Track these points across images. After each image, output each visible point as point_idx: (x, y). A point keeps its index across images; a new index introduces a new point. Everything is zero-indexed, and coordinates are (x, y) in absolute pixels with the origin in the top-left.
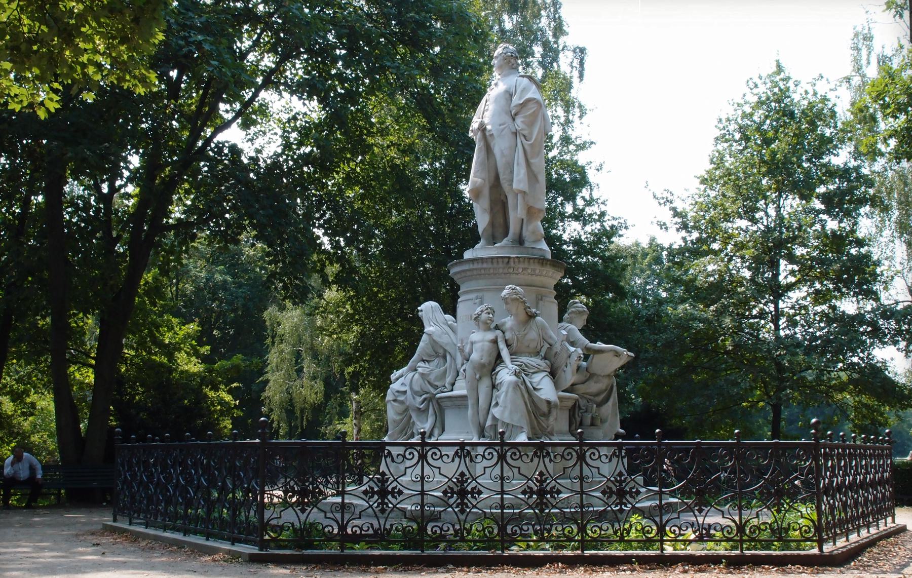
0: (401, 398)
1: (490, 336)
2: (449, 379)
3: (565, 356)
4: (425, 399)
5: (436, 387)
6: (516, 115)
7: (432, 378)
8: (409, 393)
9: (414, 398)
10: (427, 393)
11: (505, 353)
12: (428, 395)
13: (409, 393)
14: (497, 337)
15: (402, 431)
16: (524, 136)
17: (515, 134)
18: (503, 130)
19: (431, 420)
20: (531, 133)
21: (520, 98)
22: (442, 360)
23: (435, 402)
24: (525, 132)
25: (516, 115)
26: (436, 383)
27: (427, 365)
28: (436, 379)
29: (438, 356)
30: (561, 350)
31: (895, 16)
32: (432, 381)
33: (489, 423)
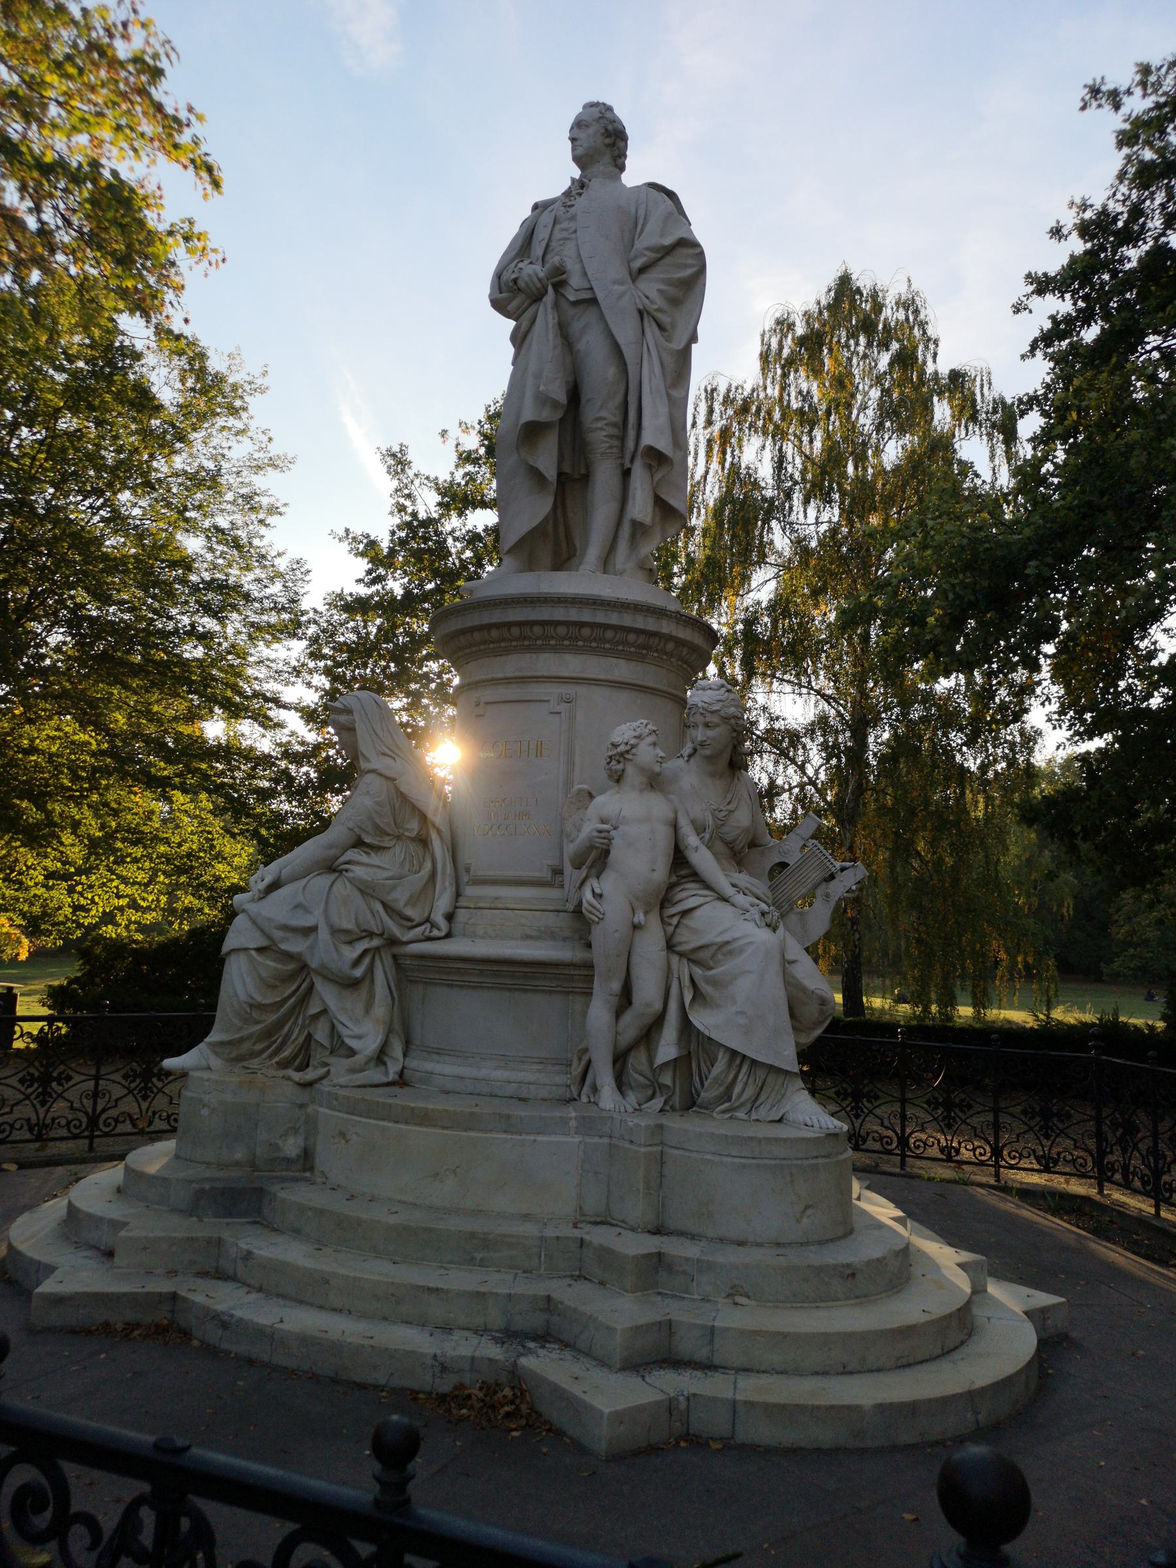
0: (295, 946)
1: (658, 806)
2: (443, 904)
3: (816, 875)
4: (365, 952)
5: (408, 923)
6: (642, 270)
7: (400, 897)
8: (323, 933)
9: (337, 950)
10: (371, 935)
11: (703, 859)
12: (376, 942)
13: (323, 933)
14: (676, 812)
15: (268, 1033)
16: (661, 327)
17: (641, 313)
18: (622, 295)
19: (380, 1010)
20: (674, 325)
21: (662, 235)
22: (413, 848)
23: (388, 959)
24: (665, 319)
25: (642, 270)
26: (409, 912)
27: (375, 859)
28: (413, 900)
29: (399, 838)
30: (803, 862)
31: (1043, 285)
32: (400, 905)
33: (667, 1048)
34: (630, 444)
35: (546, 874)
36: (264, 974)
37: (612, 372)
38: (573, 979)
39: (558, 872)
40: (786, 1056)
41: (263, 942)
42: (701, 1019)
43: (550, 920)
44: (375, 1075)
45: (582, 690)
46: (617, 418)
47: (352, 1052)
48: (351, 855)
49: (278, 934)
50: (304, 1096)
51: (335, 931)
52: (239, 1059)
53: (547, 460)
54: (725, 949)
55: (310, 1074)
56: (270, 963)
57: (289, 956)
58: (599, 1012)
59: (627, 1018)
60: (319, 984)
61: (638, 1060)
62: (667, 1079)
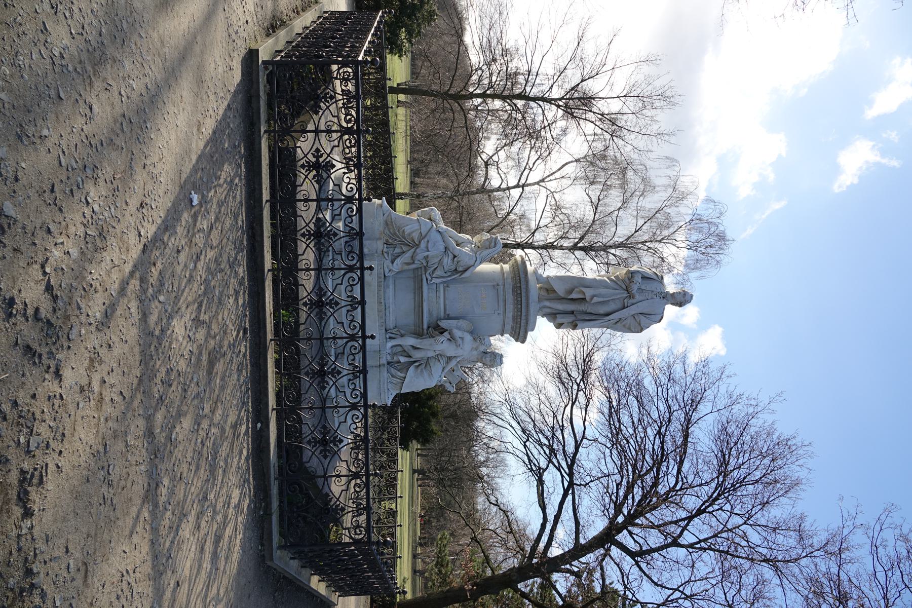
0: (423, 245)
13: (426, 254)
33: (403, 359)
34: (580, 317)
35: (447, 312)
36: (414, 234)
37: (602, 312)
38: (419, 334)
39: (448, 318)
40: (405, 390)
41: (423, 234)
42: (412, 369)
43: (435, 315)
44: (387, 270)
45: (502, 317)
46: (589, 311)
47: (393, 262)
48: (451, 256)
49: (426, 240)
50: (380, 251)
51: (428, 256)
52: (387, 224)
53: (574, 296)
54: (431, 374)
55: (385, 250)
56: (416, 236)
57: (420, 242)
58: (410, 341)
59: (411, 348)
60: (413, 250)
61: (400, 349)
62: (395, 358)
